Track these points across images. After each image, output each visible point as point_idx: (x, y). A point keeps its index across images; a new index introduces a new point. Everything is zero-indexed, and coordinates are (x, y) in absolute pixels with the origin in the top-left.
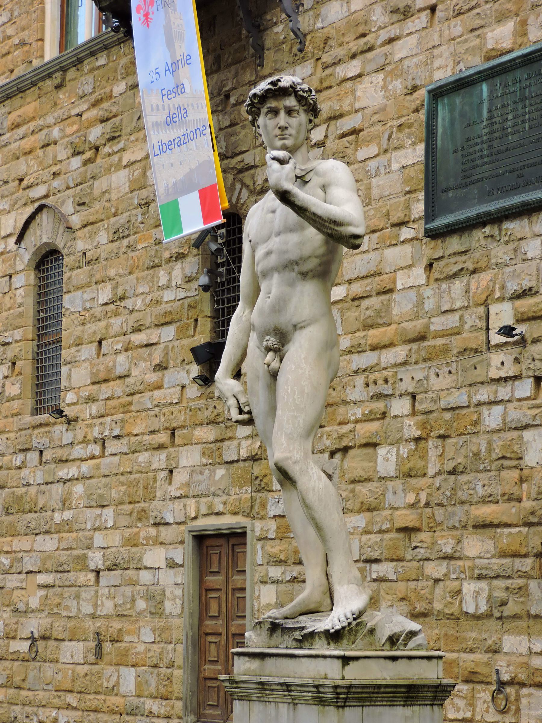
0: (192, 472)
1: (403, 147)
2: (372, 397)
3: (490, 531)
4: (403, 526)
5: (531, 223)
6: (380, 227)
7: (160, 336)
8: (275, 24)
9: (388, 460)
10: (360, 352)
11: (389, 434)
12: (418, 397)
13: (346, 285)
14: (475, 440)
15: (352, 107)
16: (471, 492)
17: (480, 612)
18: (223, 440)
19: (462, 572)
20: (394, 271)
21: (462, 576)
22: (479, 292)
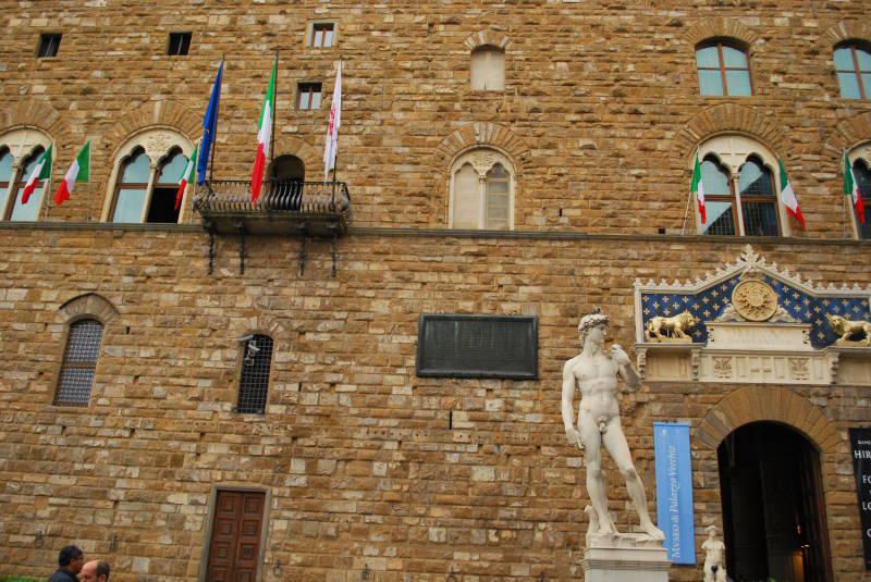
18: (249, 444)
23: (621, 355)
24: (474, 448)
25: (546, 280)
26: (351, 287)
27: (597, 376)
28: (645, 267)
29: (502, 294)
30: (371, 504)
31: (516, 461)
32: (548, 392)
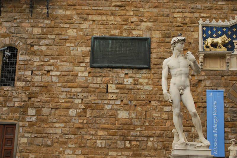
1: (82, 46)
3: (107, 130)
5: (122, 71)
8: (37, 8)
9: (73, 112)
10: (64, 87)
13: (60, 72)
14: (102, 111)
17: (102, 147)
20: (78, 72)
21: (97, 139)
22: (105, 81)
23: (191, 56)
24: (118, 102)
25: (155, 19)
26: (56, 23)
27: (179, 67)
28: (205, 13)
29: (133, 26)
30: (69, 129)
31: (139, 108)
32: (155, 75)
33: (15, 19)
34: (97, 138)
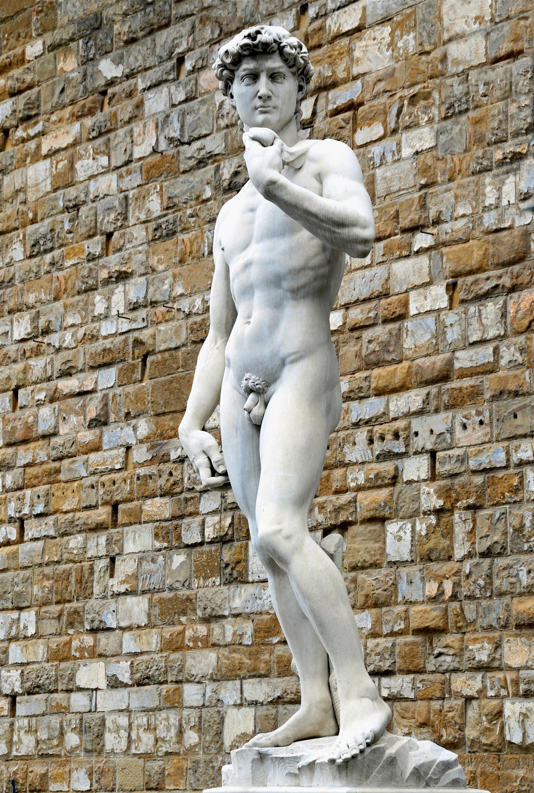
0: (141, 560)
2: (378, 457)
4: (422, 626)
6: (387, 233)
7: (96, 382)
9: (400, 539)
10: (361, 398)
11: (402, 504)
12: (439, 455)
13: (342, 311)
15: (349, 73)
16: (513, 580)
18: (182, 517)
19: (502, 687)
20: (406, 291)
21: (503, 692)
22: (519, 315)
33: (181, 61)
34: (505, 687)
